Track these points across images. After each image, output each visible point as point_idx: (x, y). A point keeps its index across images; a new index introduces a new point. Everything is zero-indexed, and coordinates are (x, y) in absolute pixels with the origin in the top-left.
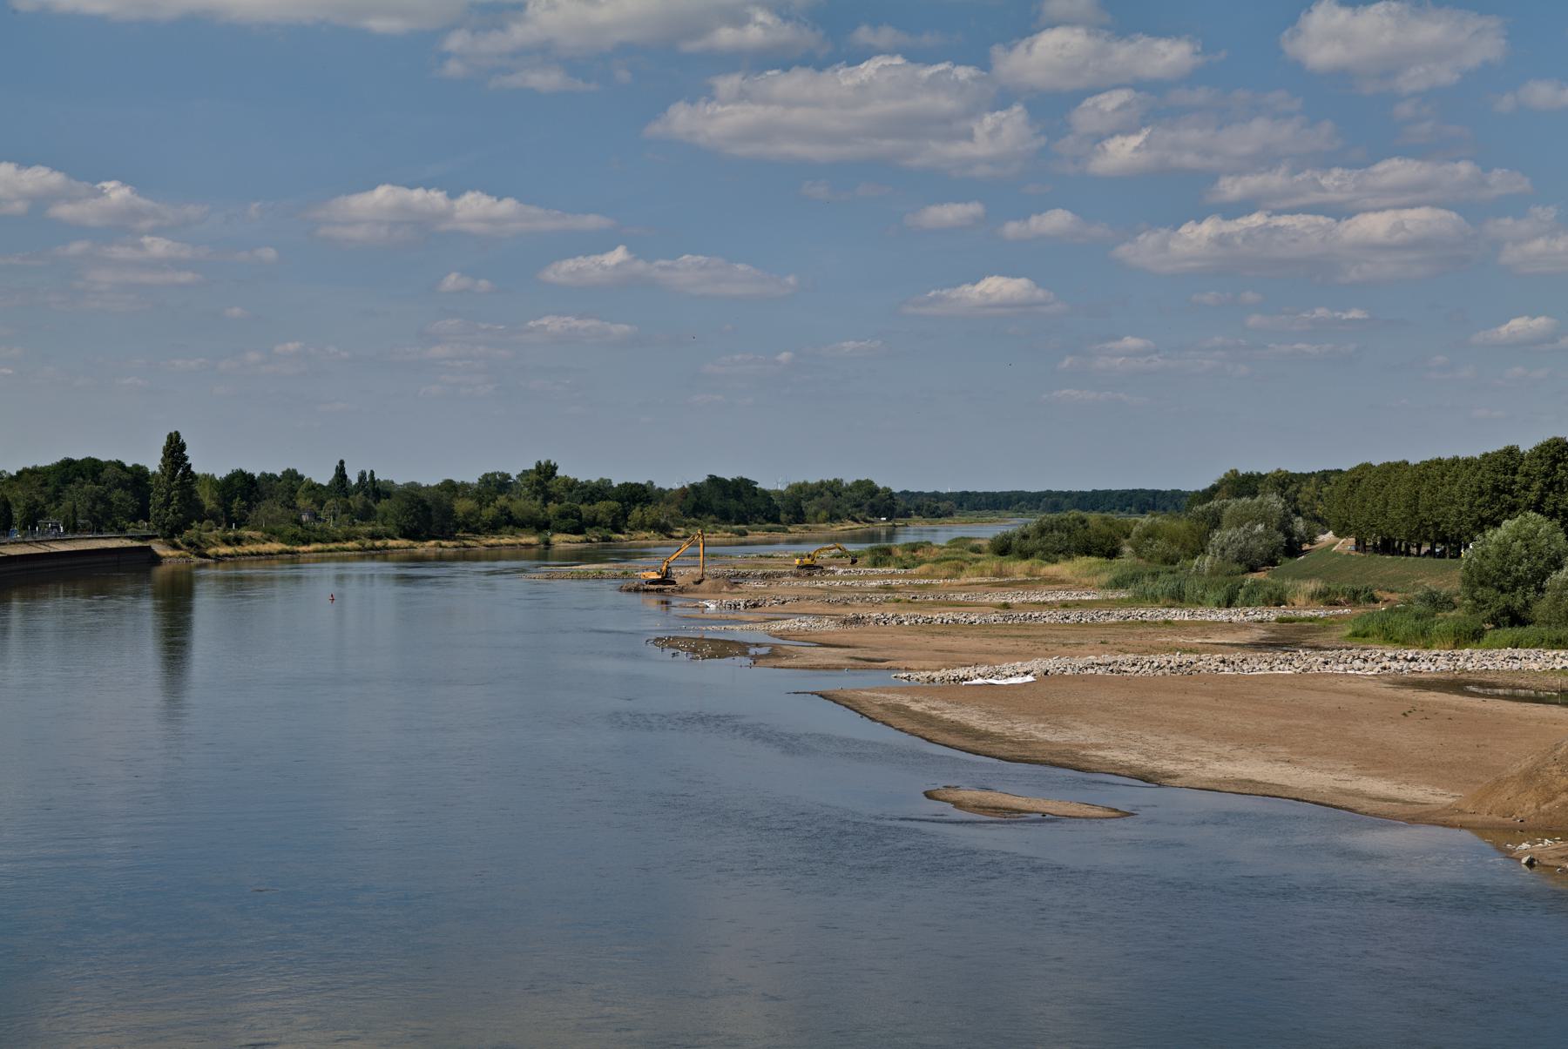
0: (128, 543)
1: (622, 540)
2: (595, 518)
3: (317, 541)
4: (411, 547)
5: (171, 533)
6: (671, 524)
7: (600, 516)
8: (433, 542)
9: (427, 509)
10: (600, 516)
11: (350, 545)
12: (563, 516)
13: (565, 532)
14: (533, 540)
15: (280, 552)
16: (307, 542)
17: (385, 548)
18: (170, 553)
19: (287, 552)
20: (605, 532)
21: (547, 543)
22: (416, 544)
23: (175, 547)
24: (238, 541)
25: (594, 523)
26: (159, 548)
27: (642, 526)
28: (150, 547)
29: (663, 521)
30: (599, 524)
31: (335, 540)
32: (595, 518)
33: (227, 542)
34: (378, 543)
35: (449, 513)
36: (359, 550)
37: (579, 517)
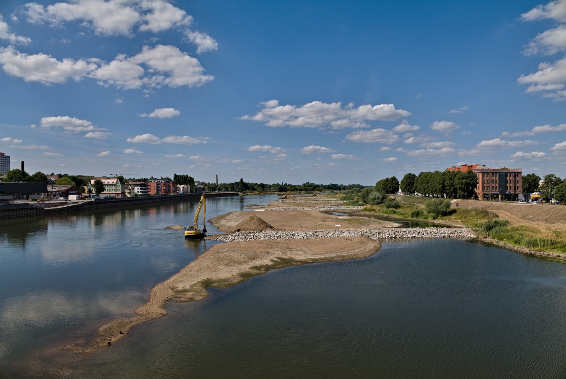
0: (235, 192)
5: (241, 191)
9: (282, 188)
11: (269, 193)
12: (304, 189)
14: (298, 192)
16: (263, 192)
18: (241, 194)
20: (310, 191)
21: (300, 193)
24: (252, 192)
25: (309, 190)
26: (239, 193)
27: (317, 190)
28: (238, 193)
33: (250, 192)
34: (274, 193)
35: (286, 189)
37: (306, 189)
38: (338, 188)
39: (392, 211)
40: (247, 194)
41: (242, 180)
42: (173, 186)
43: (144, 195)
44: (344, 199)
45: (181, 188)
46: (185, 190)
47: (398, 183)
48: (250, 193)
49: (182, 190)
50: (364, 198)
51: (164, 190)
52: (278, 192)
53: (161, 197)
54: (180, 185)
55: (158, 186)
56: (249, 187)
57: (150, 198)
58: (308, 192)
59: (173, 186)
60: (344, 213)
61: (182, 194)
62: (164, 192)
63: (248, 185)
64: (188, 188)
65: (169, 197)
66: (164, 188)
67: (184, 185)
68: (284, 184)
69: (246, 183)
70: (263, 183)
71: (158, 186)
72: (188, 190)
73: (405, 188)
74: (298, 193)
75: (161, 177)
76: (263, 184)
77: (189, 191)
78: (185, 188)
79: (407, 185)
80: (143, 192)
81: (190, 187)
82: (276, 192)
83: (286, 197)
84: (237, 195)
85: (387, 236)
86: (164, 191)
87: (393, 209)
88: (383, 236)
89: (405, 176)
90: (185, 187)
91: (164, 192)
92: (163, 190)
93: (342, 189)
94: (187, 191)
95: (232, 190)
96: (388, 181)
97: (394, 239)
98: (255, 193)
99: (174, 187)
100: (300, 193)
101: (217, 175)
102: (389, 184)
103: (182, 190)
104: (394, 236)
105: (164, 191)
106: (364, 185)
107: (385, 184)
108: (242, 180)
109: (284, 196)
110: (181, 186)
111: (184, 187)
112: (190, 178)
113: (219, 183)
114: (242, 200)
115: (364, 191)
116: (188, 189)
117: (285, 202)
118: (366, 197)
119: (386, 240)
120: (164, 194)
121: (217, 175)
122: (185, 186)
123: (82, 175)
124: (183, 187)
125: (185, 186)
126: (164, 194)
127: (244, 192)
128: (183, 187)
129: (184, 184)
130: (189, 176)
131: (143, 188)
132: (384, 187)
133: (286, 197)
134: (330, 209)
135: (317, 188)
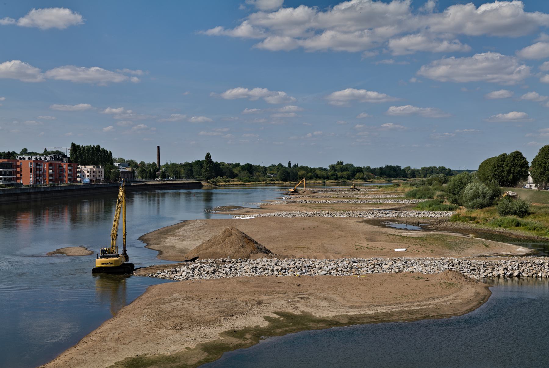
0: (194, 181)
1: (349, 182)
2: (343, 176)
3: (253, 181)
4: (282, 183)
5: (207, 179)
6: (367, 178)
7: (344, 176)
8: (288, 182)
9: (289, 173)
10: (344, 176)
11: (262, 183)
12: (332, 175)
13: (332, 180)
14: (321, 182)
15: (240, 184)
16: (250, 182)
17: (274, 183)
18: (206, 184)
19: (242, 184)
20: (345, 180)
21: (324, 182)
22: (284, 182)
23: (208, 182)
24: (229, 181)
25: (342, 177)
26: (203, 183)
27: (359, 178)
28: (201, 183)
29: (365, 177)
30: (344, 178)
31: (259, 181)
32: (343, 176)
33: (225, 182)
34: (272, 182)
35: (296, 175)
36: (265, 184)
37: (337, 176)
38: (401, 175)
39: (513, 222)
40: (218, 184)
41: (208, 156)
42: (70, 168)
43: (8, 185)
44: (413, 195)
45: (86, 172)
46: (94, 176)
47: (525, 164)
48: (224, 183)
49: (86, 177)
50: (454, 194)
51: (51, 175)
52: (280, 182)
53: (43, 190)
54: (83, 167)
55: (38, 167)
56: (223, 170)
57: (20, 192)
58: (341, 181)
59: (70, 168)
60: (413, 224)
61: (86, 184)
62: (50, 180)
63: (221, 166)
64: (99, 172)
65: (58, 191)
66: (51, 171)
67: (91, 167)
68: (292, 166)
69: (217, 162)
70: (250, 163)
71: (38, 167)
72: (99, 176)
73: (541, 174)
74: (319, 183)
75: (44, 150)
76: (251, 165)
77: (102, 178)
78: (94, 172)
79: (545, 169)
80: (5, 180)
81: (103, 170)
82: (277, 182)
83: (296, 191)
84: (200, 186)
85: (501, 272)
86: (51, 178)
87: (515, 217)
88: (494, 273)
89: (540, 150)
90: (95, 169)
91: (50, 180)
92: (47, 175)
93: (409, 176)
94: (98, 178)
95: (188, 178)
96: (504, 161)
97: (516, 279)
98: (235, 183)
99: (70, 170)
100: (324, 184)
101: (159, 147)
102: (507, 165)
103: (86, 177)
104: (516, 273)
105: (51, 178)
106: (453, 168)
107: (498, 166)
108: (208, 156)
109: (292, 190)
110: (85, 167)
111: (91, 169)
112: (105, 152)
113: (162, 164)
114: (208, 197)
115: (454, 181)
116: (100, 174)
117: (294, 202)
118: (458, 192)
119: (501, 280)
120: (49, 183)
121: (159, 147)
122: (94, 167)
123: (34, 152)
124: (89, 170)
125: (94, 167)
126: (49, 183)
127: (213, 182)
128: (89, 170)
129: (92, 165)
130: (101, 147)
131: (5, 172)
132: (496, 173)
133: (296, 191)
134: (385, 216)
135: (357, 175)
